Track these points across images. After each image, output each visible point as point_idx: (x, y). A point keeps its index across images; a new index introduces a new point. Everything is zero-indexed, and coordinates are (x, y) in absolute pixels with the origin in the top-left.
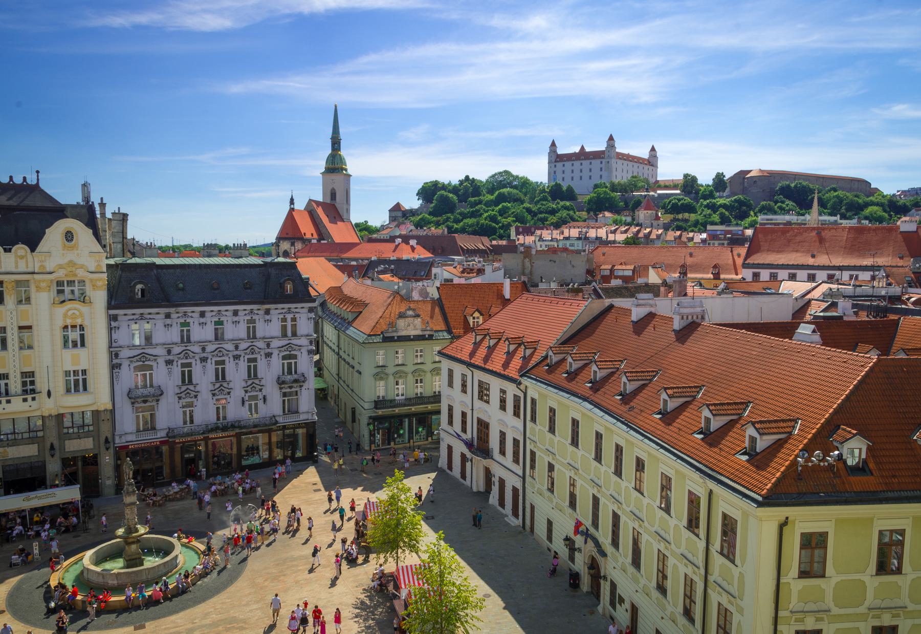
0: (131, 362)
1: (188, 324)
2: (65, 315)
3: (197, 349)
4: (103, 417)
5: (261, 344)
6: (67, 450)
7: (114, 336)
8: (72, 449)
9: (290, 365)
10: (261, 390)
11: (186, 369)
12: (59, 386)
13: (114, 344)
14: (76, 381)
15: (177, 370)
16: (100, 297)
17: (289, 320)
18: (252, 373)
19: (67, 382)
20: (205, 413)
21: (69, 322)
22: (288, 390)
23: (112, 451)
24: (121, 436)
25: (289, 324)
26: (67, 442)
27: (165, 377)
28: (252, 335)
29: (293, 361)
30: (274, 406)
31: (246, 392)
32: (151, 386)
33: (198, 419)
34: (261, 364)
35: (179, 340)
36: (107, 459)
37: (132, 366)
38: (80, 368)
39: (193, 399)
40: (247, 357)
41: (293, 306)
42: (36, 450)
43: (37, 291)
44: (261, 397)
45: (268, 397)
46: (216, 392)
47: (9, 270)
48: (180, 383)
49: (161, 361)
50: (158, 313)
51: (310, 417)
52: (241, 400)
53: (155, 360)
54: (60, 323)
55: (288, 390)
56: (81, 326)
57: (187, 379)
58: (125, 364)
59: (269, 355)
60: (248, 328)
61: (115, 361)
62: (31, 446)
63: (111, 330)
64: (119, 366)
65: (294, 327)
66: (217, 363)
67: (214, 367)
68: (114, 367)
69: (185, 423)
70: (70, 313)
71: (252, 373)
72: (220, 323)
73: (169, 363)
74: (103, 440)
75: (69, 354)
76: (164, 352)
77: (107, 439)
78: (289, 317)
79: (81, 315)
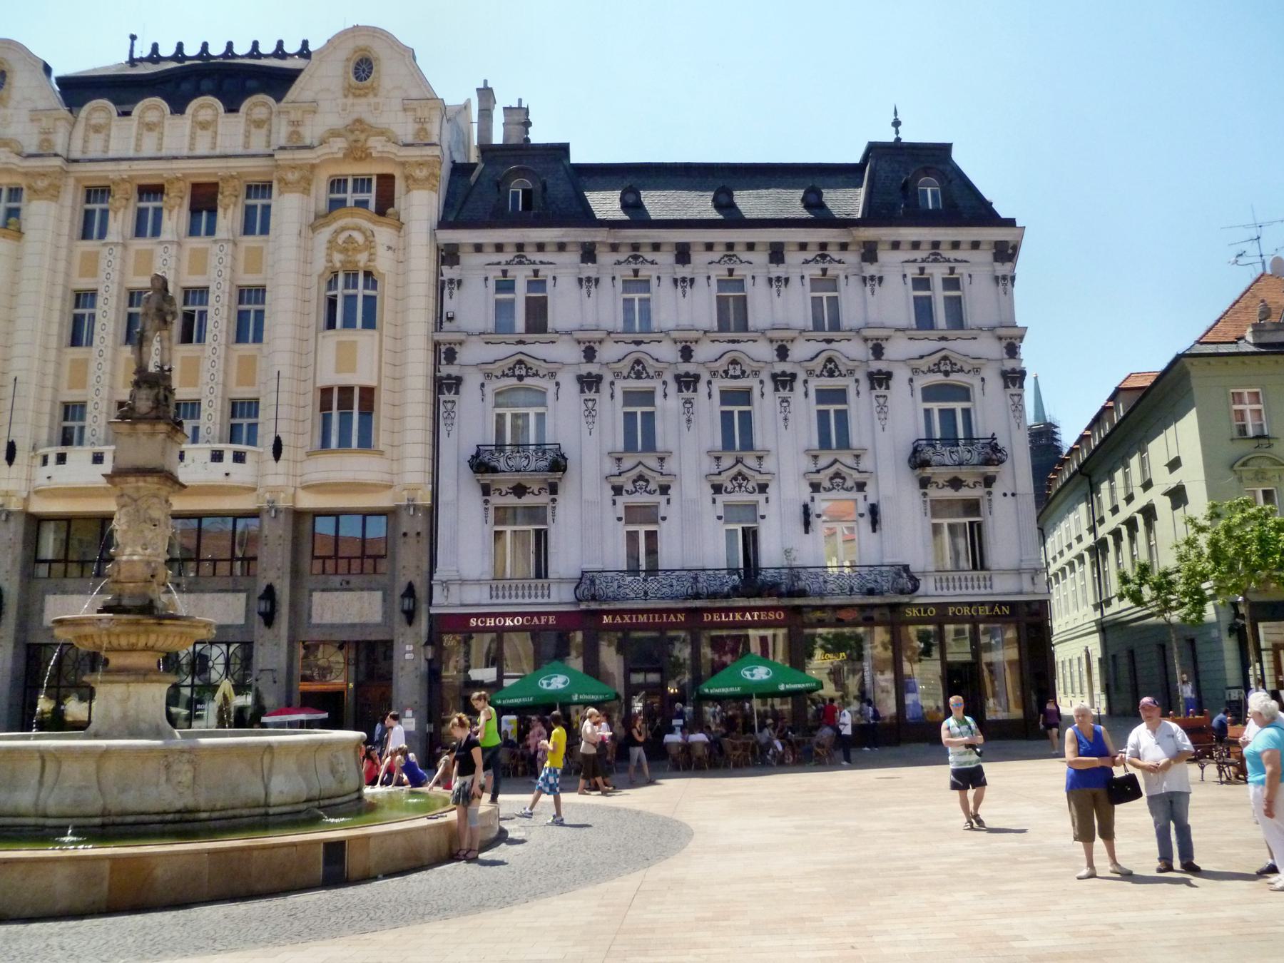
0: (488, 376)
1: (645, 285)
2: (332, 243)
3: (668, 352)
4: (406, 524)
5: (854, 350)
6: (316, 619)
7: (449, 305)
8: (328, 619)
9: (948, 415)
10: (861, 486)
11: (639, 410)
13: (446, 325)
15: (611, 410)
16: (421, 206)
17: (937, 283)
18: (833, 431)
20: (697, 541)
23: (423, 625)
24: (446, 584)
25: (939, 295)
26: (317, 596)
27: (583, 431)
28: (827, 320)
29: (958, 406)
31: (816, 487)
33: (669, 556)
34: (860, 405)
35: (620, 325)
36: (409, 656)
37: (489, 389)
38: (360, 378)
39: (658, 498)
40: (814, 384)
41: (945, 234)
43: (281, 193)
44: (863, 507)
46: (724, 479)
47: (229, 151)
48: (620, 445)
50: (561, 247)
52: (799, 511)
53: (553, 375)
54: (320, 264)
57: (640, 433)
59: (880, 380)
60: (817, 302)
61: (446, 370)
62: (230, 597)
63: (441, 287)
64: (454, 384)
66: (728, 397)
67: (717, 407)
68: (445, 385)
69: (633, 570)
70: (341, 238)
71: (833, 431)
72: (732, 282)
73: (589, 383)
76: (575, 354)
77: (410, 591)
78: (938, 272)
79: (370, 244)
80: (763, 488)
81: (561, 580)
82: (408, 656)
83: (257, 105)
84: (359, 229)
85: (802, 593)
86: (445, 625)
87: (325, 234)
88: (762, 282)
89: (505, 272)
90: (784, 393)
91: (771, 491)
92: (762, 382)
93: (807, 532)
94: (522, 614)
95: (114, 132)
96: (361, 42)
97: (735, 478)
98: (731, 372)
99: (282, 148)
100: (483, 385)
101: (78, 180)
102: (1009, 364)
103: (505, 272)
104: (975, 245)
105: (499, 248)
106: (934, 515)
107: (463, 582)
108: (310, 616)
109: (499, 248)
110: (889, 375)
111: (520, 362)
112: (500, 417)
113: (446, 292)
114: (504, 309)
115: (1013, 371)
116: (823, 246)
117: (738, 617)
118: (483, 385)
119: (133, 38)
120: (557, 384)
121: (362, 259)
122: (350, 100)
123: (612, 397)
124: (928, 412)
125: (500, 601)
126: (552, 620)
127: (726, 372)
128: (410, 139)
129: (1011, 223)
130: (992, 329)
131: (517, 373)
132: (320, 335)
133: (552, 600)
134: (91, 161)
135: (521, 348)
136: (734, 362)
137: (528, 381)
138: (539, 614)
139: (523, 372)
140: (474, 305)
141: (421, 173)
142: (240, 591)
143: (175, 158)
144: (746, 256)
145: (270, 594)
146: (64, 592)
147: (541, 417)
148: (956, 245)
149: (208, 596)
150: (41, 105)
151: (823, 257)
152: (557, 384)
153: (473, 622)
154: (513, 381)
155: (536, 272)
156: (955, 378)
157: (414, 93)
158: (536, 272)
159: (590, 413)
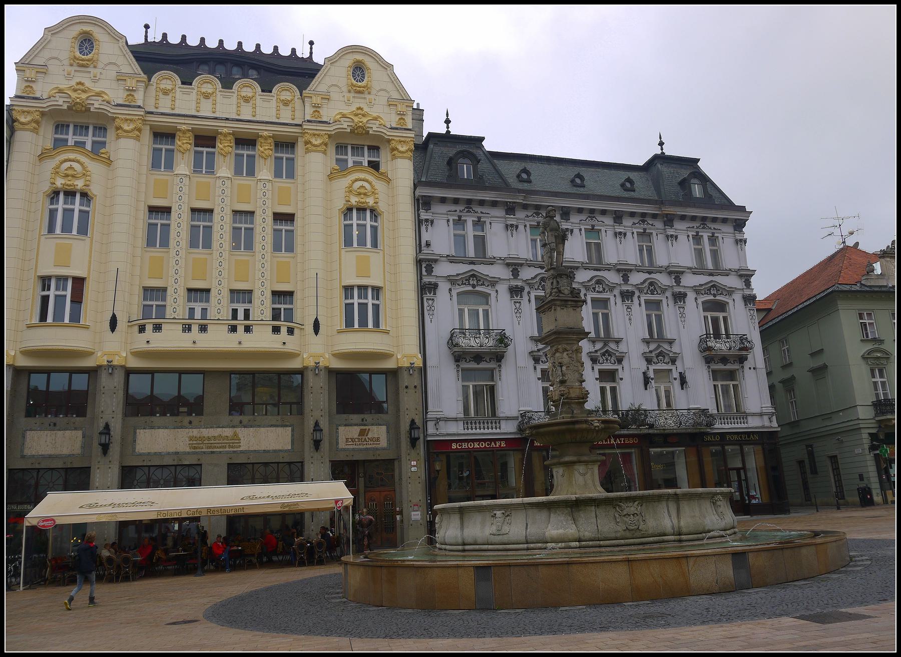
2: (350, 190)
4: (405, 380)
5: (663, 280)
7: (425, 237)
9: (715, 321)
10: (673, 361)
12: (333, 319)
13: (425, 250)
14: (363, 307)
16: (402, 170)
19: (349, 308)
21: (354, 200)
22: (720, 366)
24: (438, 420)
29: (721, 315)
30: (700, 394)
31: (649, 361)
32: (487, 330)
37: (454, 293)
42: (289, 439)
43: (308, 151)
44: (675, 374)
45: (689, 377)
49: (503, 288)
51: (767, 424)
52: (641, 376)
54: (340, 204)
55: (720, 366)
56: (372, 211)
58: (443, 287)
59: (680, 297)
61: (426, 279)
62: (280, 430)
64: (433, 287)
65: (715, 254)
68: (426, 289)
73: (515, 291)
74: (405, 426)
75: (350, 258)
80: (620, 361)
81: (508, 419)
82: (413, 469)
83: (285, 91)
84: (370, 183)
85: (651, 426)
86: (438, 449)
87: (345, 182)
88: (610, 233)
89: (460, 217)
90: (628, 302)
91: (625, 363)
92: (615, 296)
93: (646, 389)
94: (485, 440)
95: (178, 94)
96: (359, 57)
97: (604, 354)
98: (597, 289)
99: (308, 121)
100: (450, 290)
101: (152, 127)
102: (747, 292)
103: (460, 217)
104: (725, 221)
105: (456, 201)
106: (714, 380)
107: (447, 420)
108: (337, 443)
109: (456, 201)
110: (685, 295)
111: (473, 276)
112: (461, 311)
113: (423, 228)
114: (460, 240)
115: (750, 296)
116: (644, 215)
117: (612, 441)
118: (450, 290)
119: (147, 27)
120: (497, 291)
121: (370, 201)
122: (352, 95)
123: (529, 301)
124: (706, 318)
125: (470, 431)
126: (503, 444)
127: (594, 289)
128: (394, 126)
129: (742, 209)
130: (737, 271)
131: (471, 283)
132: (343, 252)
133: (502, 431)
134: (163, 114)
135: (472, 267)
136: (599, 282)
137: (477, 288)
138: (495, 440)
139: (475, 283)
140: (441, 237)
141: (403, 148)
142: (286, 426)
143: (227, 119)
144: (600, 218)
145: (317, 428)
146: (152, 428)
147: (486, 313)
148: (714, 220)
149: (262, 429)
150: (126, 69)
151: (643, 221)
152: (497, 291)
153: (454, 446)
154: (470, 288)
155: (479, 218)
156: (718, 298)
157: (395, 95)
158: (479, 218)
159: (518, 311)
